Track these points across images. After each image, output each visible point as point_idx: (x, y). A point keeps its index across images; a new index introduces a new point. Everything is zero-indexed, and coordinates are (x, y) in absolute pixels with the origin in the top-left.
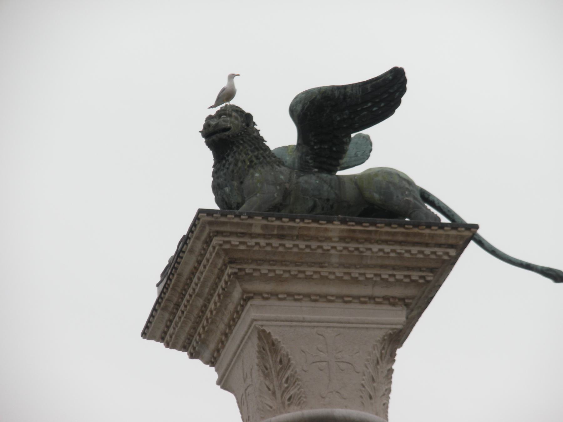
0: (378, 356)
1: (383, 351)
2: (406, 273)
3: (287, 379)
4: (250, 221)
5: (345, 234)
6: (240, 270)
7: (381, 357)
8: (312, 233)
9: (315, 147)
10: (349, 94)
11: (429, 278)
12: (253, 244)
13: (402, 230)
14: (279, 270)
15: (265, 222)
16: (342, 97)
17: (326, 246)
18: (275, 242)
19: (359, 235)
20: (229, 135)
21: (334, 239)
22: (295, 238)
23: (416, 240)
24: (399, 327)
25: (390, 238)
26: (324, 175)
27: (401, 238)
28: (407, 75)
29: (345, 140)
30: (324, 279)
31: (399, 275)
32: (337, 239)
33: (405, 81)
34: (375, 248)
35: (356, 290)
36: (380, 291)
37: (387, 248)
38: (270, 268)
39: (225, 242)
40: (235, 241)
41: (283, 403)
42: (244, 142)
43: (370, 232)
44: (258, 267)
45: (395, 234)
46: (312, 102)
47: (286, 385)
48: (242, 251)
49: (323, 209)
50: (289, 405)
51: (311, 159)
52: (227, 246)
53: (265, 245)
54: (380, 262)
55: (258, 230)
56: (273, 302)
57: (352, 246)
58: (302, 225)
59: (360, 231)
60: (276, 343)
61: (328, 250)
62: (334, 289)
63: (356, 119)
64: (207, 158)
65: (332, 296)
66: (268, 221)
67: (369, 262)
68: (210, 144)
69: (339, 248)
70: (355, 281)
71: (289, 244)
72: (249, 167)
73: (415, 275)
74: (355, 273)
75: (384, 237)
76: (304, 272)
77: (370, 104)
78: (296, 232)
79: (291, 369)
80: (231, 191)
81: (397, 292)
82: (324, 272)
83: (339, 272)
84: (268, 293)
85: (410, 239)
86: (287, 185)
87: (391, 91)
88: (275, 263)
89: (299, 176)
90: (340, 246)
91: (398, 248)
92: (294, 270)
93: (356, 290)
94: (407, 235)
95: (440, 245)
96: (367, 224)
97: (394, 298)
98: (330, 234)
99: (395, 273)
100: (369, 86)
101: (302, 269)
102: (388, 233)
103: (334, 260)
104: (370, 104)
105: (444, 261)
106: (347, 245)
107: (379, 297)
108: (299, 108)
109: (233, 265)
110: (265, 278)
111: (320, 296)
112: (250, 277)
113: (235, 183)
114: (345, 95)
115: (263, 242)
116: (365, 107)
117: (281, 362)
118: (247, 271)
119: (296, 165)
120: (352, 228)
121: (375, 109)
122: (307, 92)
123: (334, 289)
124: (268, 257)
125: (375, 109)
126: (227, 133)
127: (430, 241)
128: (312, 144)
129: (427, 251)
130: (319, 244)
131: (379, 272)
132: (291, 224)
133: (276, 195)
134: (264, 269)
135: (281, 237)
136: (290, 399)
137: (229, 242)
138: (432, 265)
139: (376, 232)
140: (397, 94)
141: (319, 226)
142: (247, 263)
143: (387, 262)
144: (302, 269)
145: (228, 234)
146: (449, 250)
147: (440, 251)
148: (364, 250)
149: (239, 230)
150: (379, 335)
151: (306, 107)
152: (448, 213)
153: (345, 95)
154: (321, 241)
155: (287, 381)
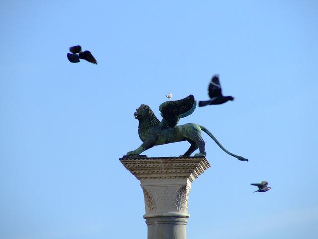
14: (146, 172)
20: (143, 115)
26: (171, 129)
30: (162, 173)
31: (183, 171)
34: (175, 164)
37: (178, 164)
52: (130, 167)
56: (146, 180)
57: (168, 164)
70: (171, 173)
73: (188, 170)
74: (170, 171)
82: (160, 171)
83: (165, 171)
88: (145, 170)
89: (162, 130)
90: (164, 165)
92: (151, 171)
95: (195, 162)
110: (143, 174)
112: (139, 174)
115: (140, 165)
122: (164, 103)
129: (191, 164)
134: (142, 172)
150: (179, 188)
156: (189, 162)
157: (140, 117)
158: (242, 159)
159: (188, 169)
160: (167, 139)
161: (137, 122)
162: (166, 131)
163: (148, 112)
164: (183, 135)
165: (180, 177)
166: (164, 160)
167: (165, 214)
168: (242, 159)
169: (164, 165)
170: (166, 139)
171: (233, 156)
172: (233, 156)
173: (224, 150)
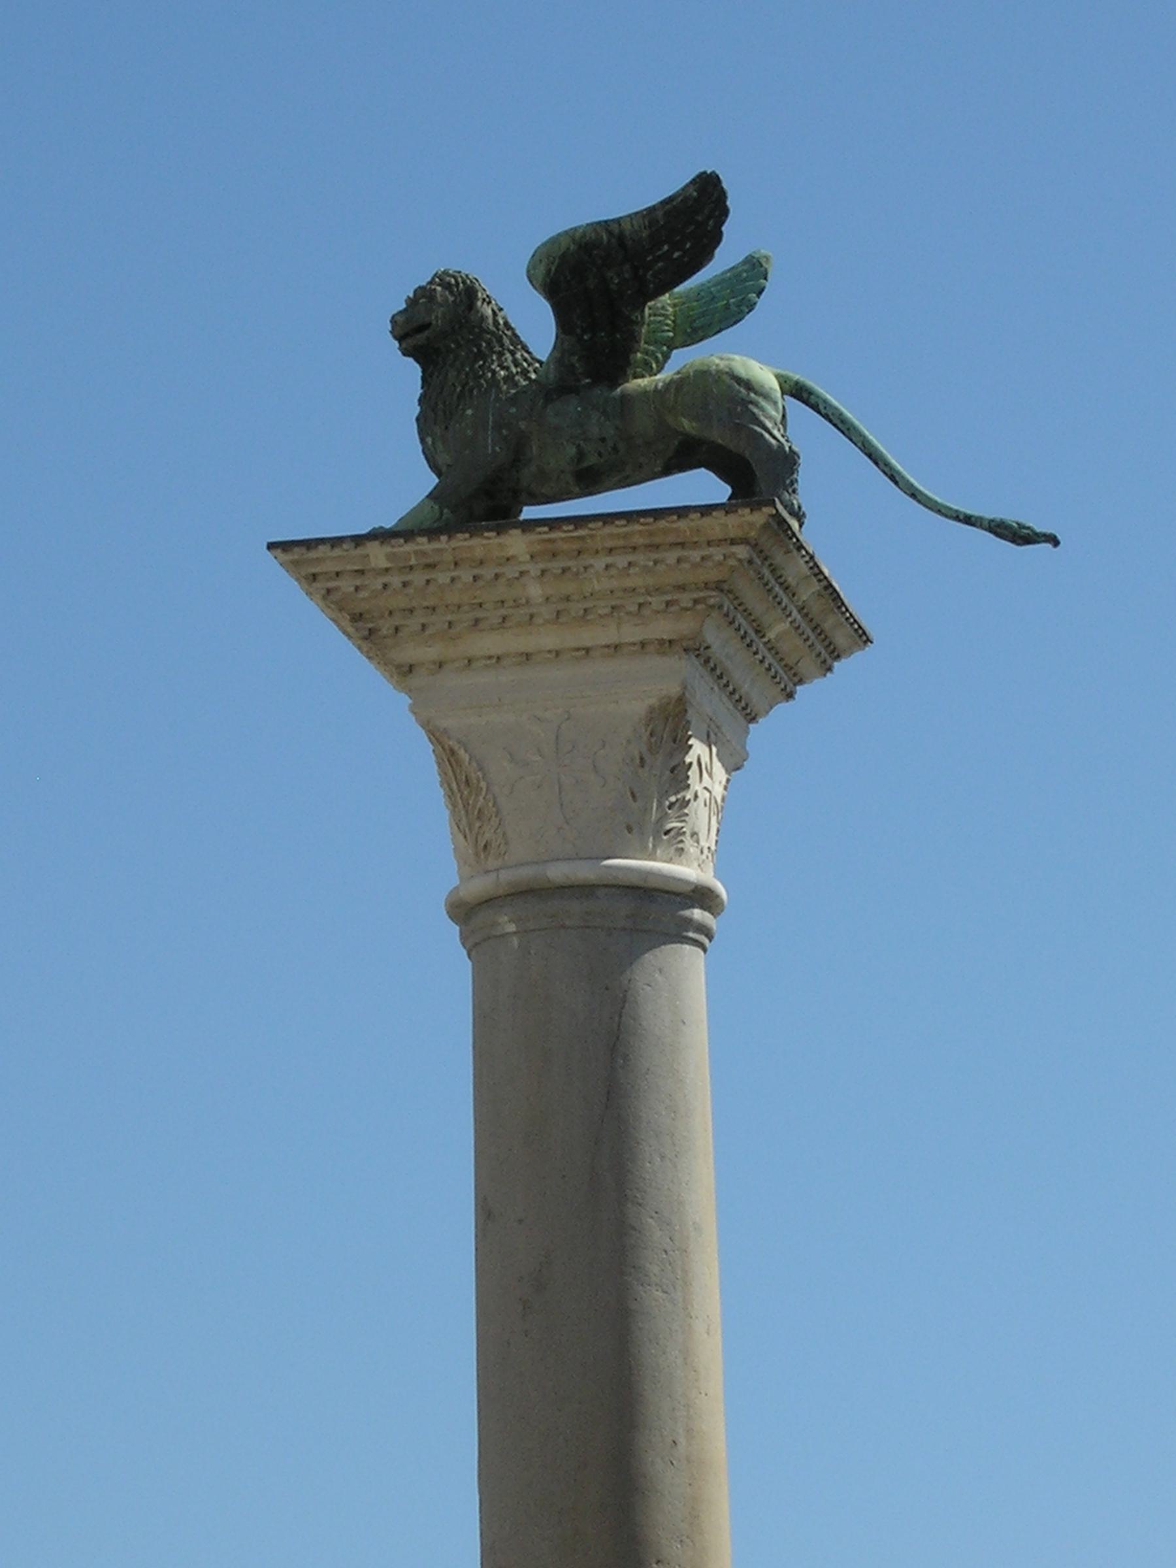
0: (644, 749)
1: (653, 740)
2: (668, 598)
3: (480, 810)
4: (360, 551)
5: (538, 547)
6: (371, 631)
7: (650, 750)
8: (479, 553)
9: (586, 337)
10: (627, 233)
11: (712, 601)
12: (380, 587)
13: (638, 527)
15: (387, 549)
16: (613, 240)
17: (510, 572)
18: (418, 578)
19: (565, 546)
20: (442, 330)
21: (521, 559)
22: (452, 566)
23: (671, 538)
24: (674, 690)
25: (621, 543)
27: (640, 541)
28: (725, 185)
29: (633, 318)
31: (657, 602)
32: (528, 557)
33: (723, 195)
34: (599, 563)
35: (589, 636)
36: (631, 633)
37: (621, 561)
38: (423, 620)
39: (329, 591)
40: (346, 585)
41: (477, 854)
42: (459, 346)
43: (581, 538)
44: (402, 622)
45: (625, 536)
46: (563, 256)
47: (478, 824)
48: (363, 599)
49: (600, 455)
50: (486, 858)
51: (579, 360)
53: (400, 585)
54: (615, 583)
55: (383, 563)
57: (556, 566)
58: (454, 543)
59: (563, 539)
60: (456, 748)
61: (517, 579)
62: (549, 639)
63: (648, 277)
64: (408, 375)
65: (549, 652)
66: (393, 547)
67: (597, 588)
68: (406, 353)
69: (532, 573)
71: (443, 578)
72: (461, 397)
73: (685, 599)
75: (610, 544)
76: (486, 618)
77: (666, 248)
78: (448, 557)
79: (483, 793)
80: (433, 443)
81: (663, 628)
84: (434, 663)
85: (657, 540)
86: (522, 425)
87: (699, 218)
91: (641, 558)
93: (589, 636)
94: (651, 534)
95: (720, 542)
96: (571, 527)
97: (661, 642)
98: (511, 552)
99: (650, 599)
100: (660, 214)
101: (480, 614)
102: (611, 536)
103: (535, 591)
104: (666, 248)
105: (733, 569)
106: (549, 565)
107: (634, 644)
108: (541, 270)
109: (360, 624)
111: (528, 656)
113: (438, 430)
114: (653, 223)
115: (396, 580)
116: (660, 253)
117: (467, 782)
118: (384, 632)
119: (551, 376)
120: (546, 536)
121: (676, 255)
122: (553, 241)
123: (549, 639)
124: (414, 604)
125: (676, 255)
126: (426, 333)
127: (696, 539)
128: (579, 331)
129: (695, 555)
130: (497, 571)
131: (618, 602)
132: (436, 545)
133: (497, 449)
134: (414, 623)
135: (431, 566)
136: (485, 846)
137: (337, 589)
138: (713, 575)
139: (592, 536)
140: (711, 222)
141: (485, 542)
142: (382, 617)
143: (629, 583)
144: (480, 614)
145: (333, 575)
146: (734, 549)
147: (717, 553)
148: (582, 570)
149: (349, 567)
151: (553, 269)
152: (840, 426)
153: (621, 238)
154: (500, 565)
155: (479, 818)
156: (682, 545)
157: (421, 338)
158: (1020, 536)
159: (682, 588)
160: (581, 455)
161: (412, 371)
162: (573, 406)
163: (471, 306)
164: (670, 420)
165: (643, 645)
166: (533, 537)
167: (558, 872)
168: (1020, 536)
169: (534, 570)
170: (572, 451)
171: (968, 520)
172: (968, 520)
173: (914, 494)
